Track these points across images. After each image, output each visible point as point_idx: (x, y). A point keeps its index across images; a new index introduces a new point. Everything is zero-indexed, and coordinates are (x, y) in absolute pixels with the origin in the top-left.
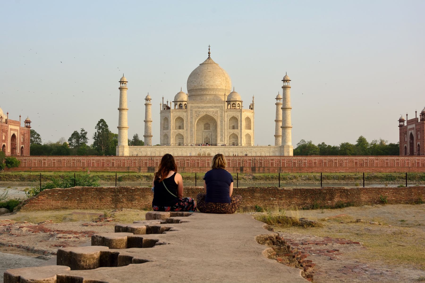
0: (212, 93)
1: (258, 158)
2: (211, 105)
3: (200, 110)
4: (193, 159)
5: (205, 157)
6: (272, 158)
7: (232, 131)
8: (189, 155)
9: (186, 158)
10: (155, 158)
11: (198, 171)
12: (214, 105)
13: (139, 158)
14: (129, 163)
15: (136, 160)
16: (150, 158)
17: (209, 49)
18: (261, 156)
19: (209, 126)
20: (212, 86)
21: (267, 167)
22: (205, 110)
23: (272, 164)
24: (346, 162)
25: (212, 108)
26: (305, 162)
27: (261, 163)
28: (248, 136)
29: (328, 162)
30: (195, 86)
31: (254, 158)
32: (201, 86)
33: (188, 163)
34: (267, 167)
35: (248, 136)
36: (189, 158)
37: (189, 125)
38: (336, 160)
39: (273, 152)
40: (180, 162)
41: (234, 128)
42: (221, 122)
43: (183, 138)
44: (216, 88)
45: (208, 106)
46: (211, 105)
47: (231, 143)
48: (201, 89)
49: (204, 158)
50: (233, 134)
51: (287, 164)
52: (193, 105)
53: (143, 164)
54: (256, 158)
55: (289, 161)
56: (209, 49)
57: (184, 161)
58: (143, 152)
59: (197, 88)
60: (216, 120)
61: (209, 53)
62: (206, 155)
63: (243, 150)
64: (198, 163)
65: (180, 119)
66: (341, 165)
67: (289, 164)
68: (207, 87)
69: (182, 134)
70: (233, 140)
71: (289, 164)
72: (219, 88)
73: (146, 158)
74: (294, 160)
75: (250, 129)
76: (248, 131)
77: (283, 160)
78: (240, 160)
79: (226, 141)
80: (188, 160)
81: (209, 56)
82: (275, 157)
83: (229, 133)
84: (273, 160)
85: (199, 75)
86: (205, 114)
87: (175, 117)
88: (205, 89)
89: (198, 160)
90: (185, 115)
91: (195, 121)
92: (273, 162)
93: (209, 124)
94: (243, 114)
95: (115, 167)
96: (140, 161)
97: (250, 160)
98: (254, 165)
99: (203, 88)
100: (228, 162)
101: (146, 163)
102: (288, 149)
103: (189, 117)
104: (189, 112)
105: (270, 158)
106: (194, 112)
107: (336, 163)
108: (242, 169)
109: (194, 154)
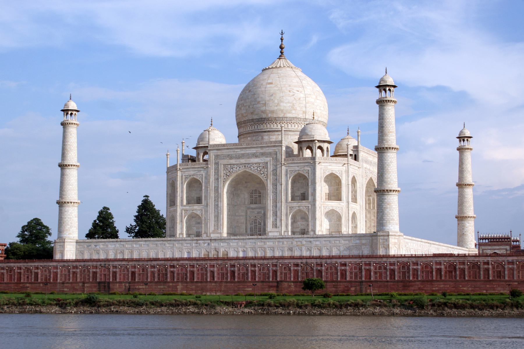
0: (274, 127)
1: (314, 261)
2: (253, 151)
3: (233, 161)
4: (183, 266)
5: (217, 259)
6: (343, 261)
7: (296, 205)
8: (186, 256)
9: (169, 263)
10: (111, 263)
11: (192, 290)
12: (260, 150)
13: (82, 264)
14: (105, 275)
15: (76, 267)
16: (103, 264)
17: (282, 39)
18: (319, 257)
19: (260, 196)
20: (272, 112)
21: (333, 282)
22: (243, 161)
23: (344, 274)
24: (512, 269)
25: (256, 157)
26: (416, 270)
27: (320, 272)
28: (335, 217)
29: (469, 268)
30: (242, 114)
31: (304, 261)
32: (252, 113)
33: (173, 272)
34: (333, 282)
35: (335, 217)
36: (175, 263)
37: (212, 194)
38: (487, 263)
39: (349, 248)
40: (159, 271)
41: (304, 197)
42: (275, 185)
43: (200, 223)
44: (281, 115)
45: (248, 154)
46: (253, 151)
47: (298, 230)
48: (252, 120)
49: (204, 262)
50: (300, 211)
51: (375, 273)
52: (219, 153)
53: (89, 276)
54: (309, 261)
55: (380, 268)
56: (282, 39)
57: (166, 270)
58: (101, 252)
59: (247, 118)
60: (265, 182)
61: (281, 48)
62: (221, 255)
63: (295, 243)
64: (192, 273)
65: (194, 184)
66: (499, 275)
67: (381, 274)
68: (264, 116)
69: (199, 213)
70: (301, 224)
71: (381, 274)
72: (289, 115)
73: (95, 263)
74: (391, 264)
75: (339, 199)
76: (334, 205)
77: (366, 264)
78: (276, 266)
79: (286, 227)
80: (173, 267)
81: (282, 53)
82: (349, 257)
83: (291, 208)
84: (345, 265)
85: (250, 91)
86: (242, 169)
87: (186, 178)
88: (262, 121)
89: (193, 266)
90: (204, 176)
91: (224, 186)
92: (345, 271)
93: (260, 193)
94: (318, 168)
95: (39, 283)
96: (84, 270)
97: (297, 265)
98: (305, 275)
99: (255, 117)
100: (252, 271)
101: (95, 273)
102: (387, 240)
103: (212, 179)
104: (212, 167)
105: (339, 261)
106: (221, 168)
107: (487, 270)
108: (278, 285)
109: (195, 255)
